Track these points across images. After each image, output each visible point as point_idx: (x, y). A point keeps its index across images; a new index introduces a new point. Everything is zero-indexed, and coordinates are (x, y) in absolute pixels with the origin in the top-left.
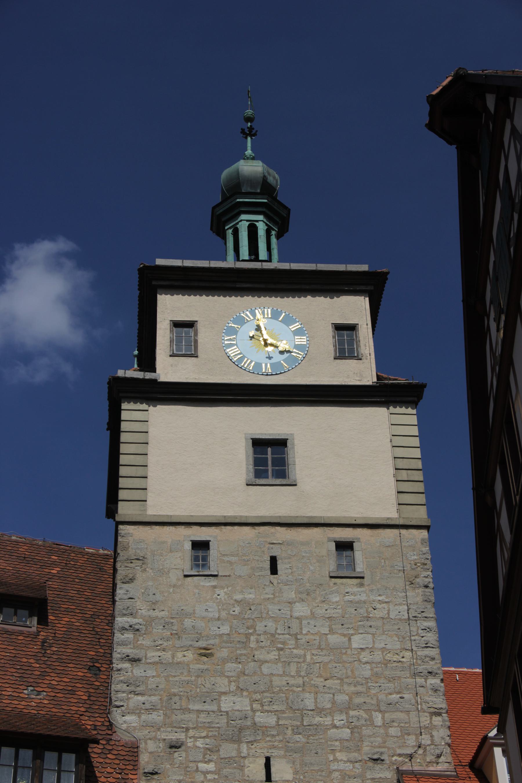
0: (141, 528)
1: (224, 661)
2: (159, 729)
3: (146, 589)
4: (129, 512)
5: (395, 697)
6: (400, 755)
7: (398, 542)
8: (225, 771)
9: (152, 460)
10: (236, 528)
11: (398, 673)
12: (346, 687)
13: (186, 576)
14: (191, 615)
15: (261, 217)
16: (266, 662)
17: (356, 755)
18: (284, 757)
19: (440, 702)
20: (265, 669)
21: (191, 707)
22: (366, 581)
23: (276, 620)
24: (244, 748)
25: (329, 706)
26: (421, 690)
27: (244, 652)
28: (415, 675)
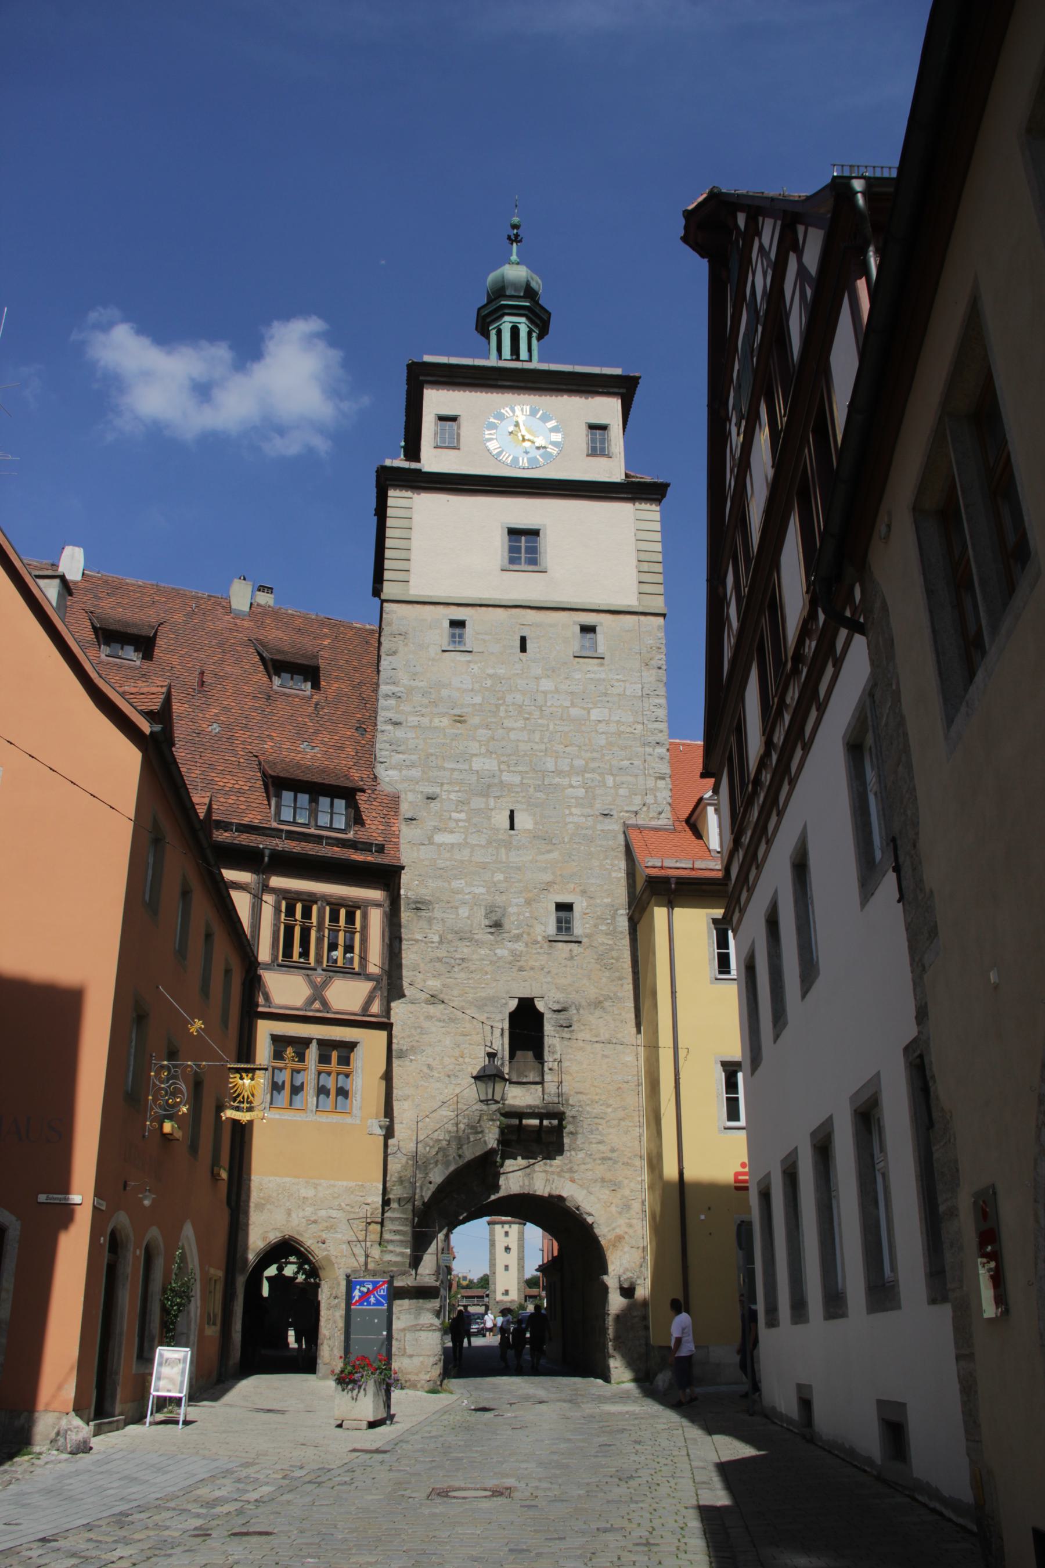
2: (417, 783)
5: (626, 763)
6: (627, 812)
7: (637, 628)
8: (475, 820)
9: (415, 544)
10: (490, 609)
12: (583, 753)
13: (444, 651)
15: (523, 320)
16: (513, 729)
17: (589, 810)
19: (665, 768)
20: (513, 735)
21: (446, 765)
22: (605, 661)
24: (492, 802)
25: (567, 769)
26: (649, 758)
27: (493, 720)
28: (644, 745)
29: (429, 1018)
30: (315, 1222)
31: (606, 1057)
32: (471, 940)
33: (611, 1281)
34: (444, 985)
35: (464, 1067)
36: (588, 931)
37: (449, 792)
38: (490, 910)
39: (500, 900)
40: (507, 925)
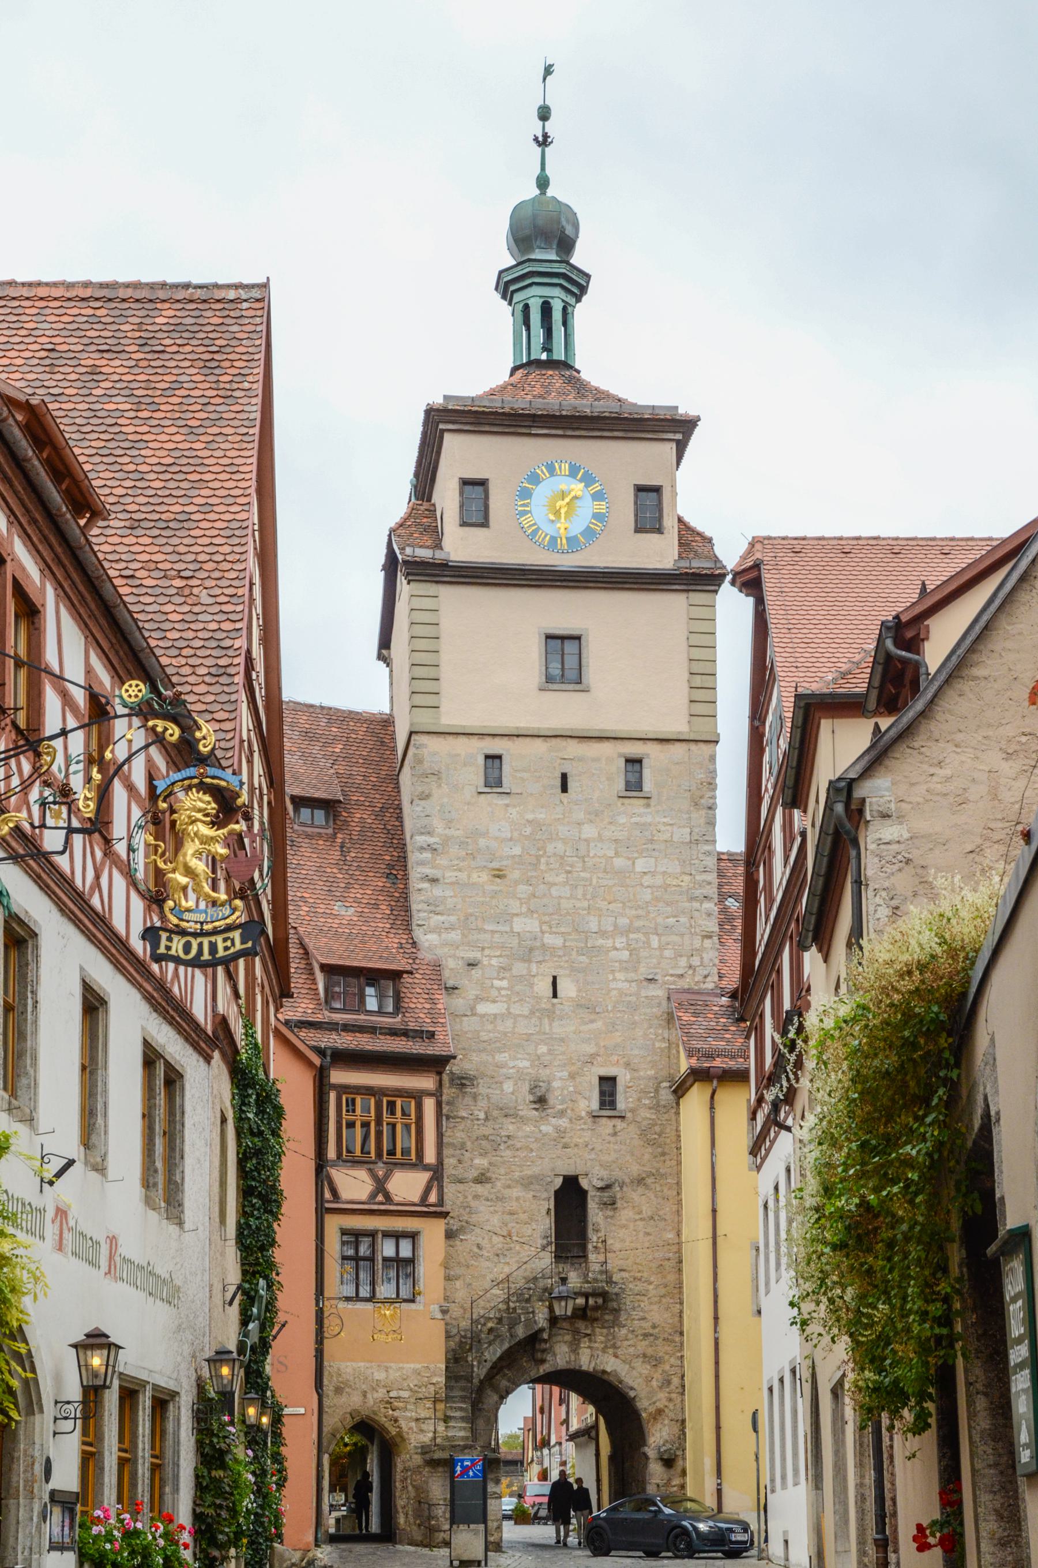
1: (516, 883)
3: (442, 806)
8: (517, 988)
10: (528, 739)
12: (627, 911)
14: (485, 834)
18: (569, 976)
20: (554, 892)
21: (486, 927)
22: (652, 802)
23: (565, 841)
24: (534, 967)
28: (693, 899)
29: (476, 1197)
31: (648, 1234)
33: (651, 1452)
34: (490, 1164)
36: (631, 1105)
39: (544, 1073)
40: (552, 1101)
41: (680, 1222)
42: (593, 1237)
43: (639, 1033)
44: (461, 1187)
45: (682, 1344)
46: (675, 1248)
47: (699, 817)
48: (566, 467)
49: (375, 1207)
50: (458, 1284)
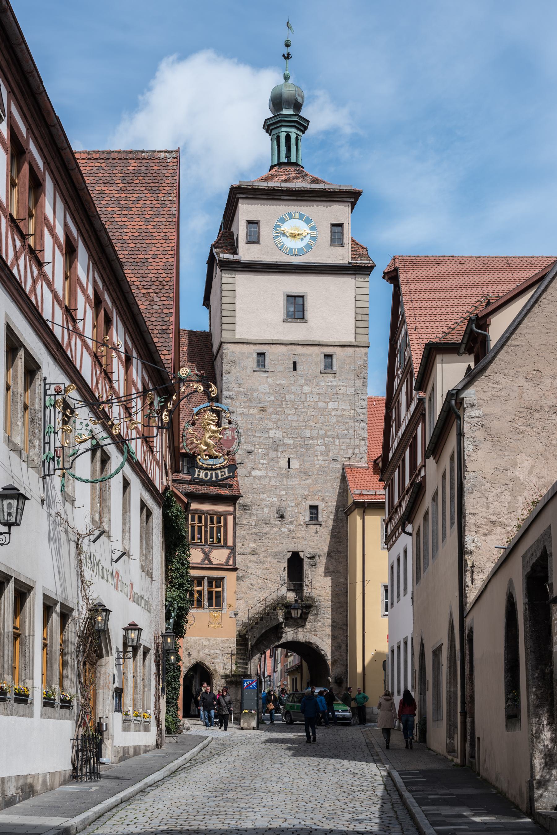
0: (233, 345)
1: (271, 414)
3: (236, 377)
4: (228, 337)
6: (345, 458)
7: (353, 355)
8: (271, 464)
9: (238, 307)
11: (348, 421)
12: (324, 427)
13: (254, 371)
16: (290, 414)
19: (365, 434)
21: (256, 435)
22: (337, 375)
23: (294, 394)
24: (279, 454)
25: (316, 435)
28: (355, 421)
29: (251, 561)
30: (209, 655)
32: (270, 524)
35: (267, 584)
36: (325, 519)
37: (259, 449)
38: (279, 510)
39: (283, 504)
41: (347, 574)
42: (306, 581)
43: (329, 485)
44: (243, 557)
45: (347, 630)
46: (345, 586)
47: (359, 383)
48: (297, 215)
49: (204, 566)
50: (241, 601)
